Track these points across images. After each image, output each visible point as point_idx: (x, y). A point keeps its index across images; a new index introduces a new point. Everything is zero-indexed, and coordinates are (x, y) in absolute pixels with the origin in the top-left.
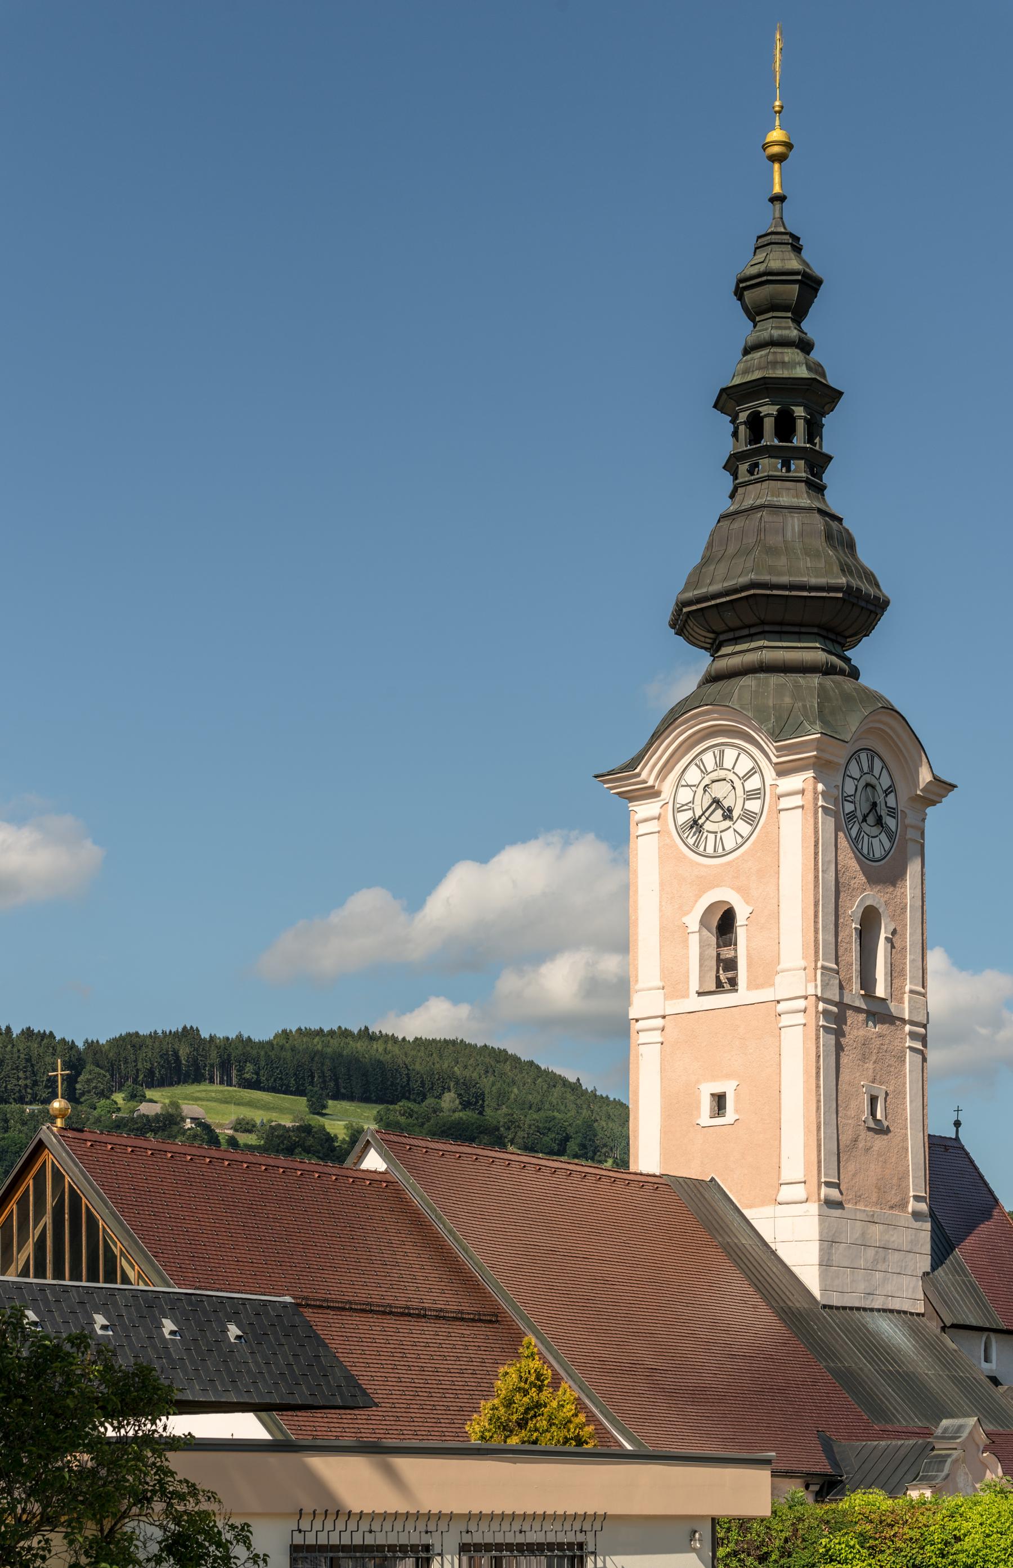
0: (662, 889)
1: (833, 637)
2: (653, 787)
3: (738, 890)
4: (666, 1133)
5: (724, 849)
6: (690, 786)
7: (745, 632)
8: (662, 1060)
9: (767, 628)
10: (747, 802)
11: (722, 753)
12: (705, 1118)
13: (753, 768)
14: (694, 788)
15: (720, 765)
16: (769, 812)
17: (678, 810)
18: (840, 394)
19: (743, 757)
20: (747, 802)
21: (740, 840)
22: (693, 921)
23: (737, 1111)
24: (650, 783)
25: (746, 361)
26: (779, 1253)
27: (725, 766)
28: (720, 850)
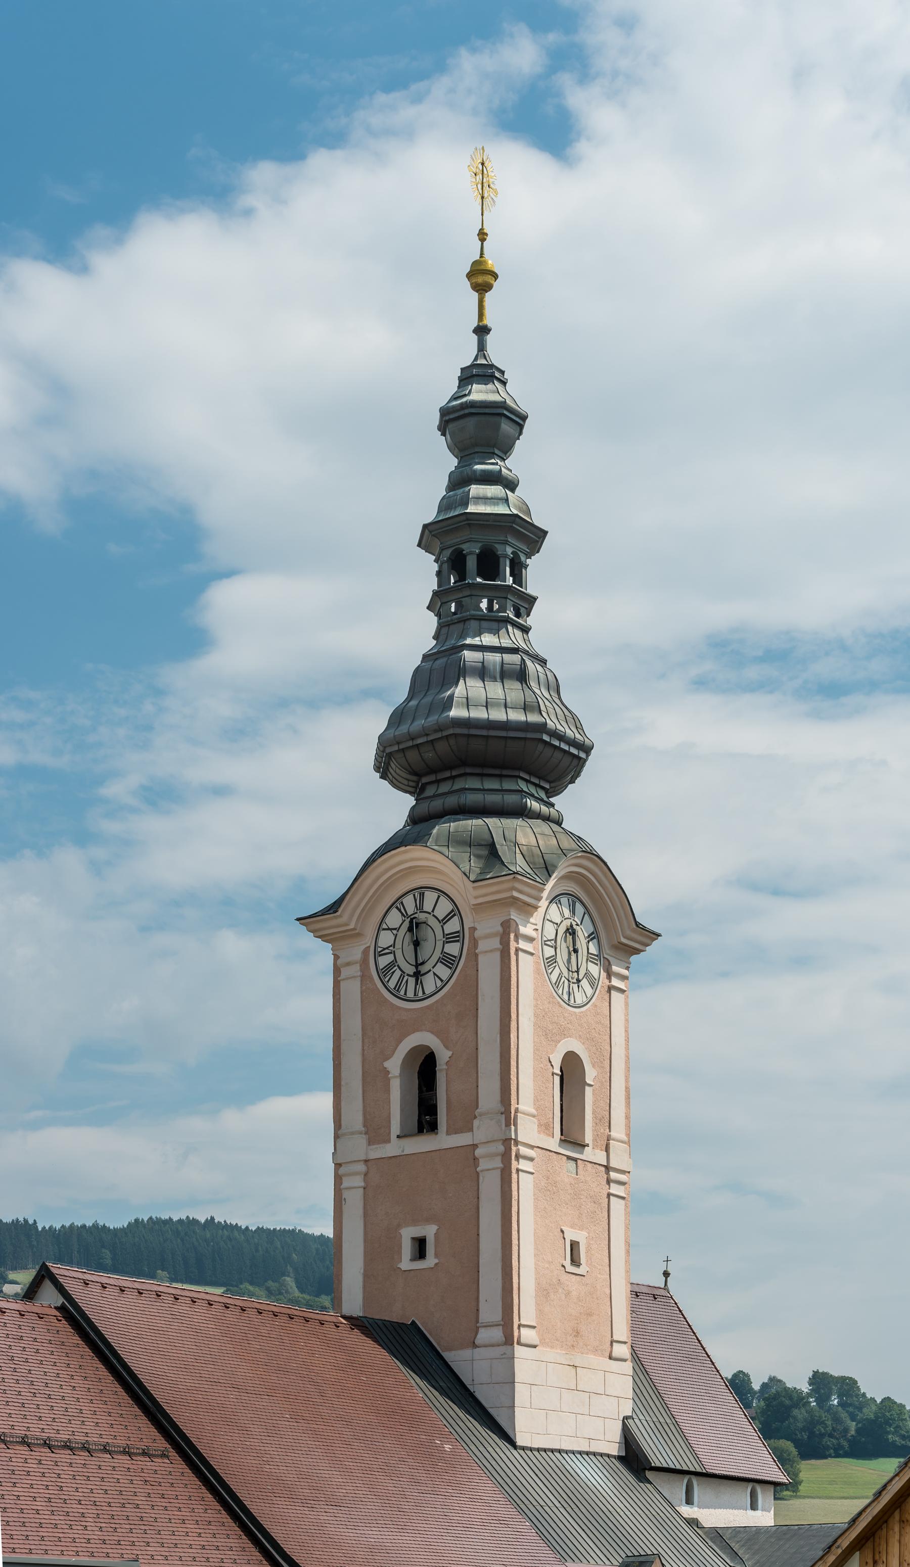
0: (364, 1034)
1: (537, 781)
2: (354, 929)
3: (437, 1034)
4: (368, 1276)
5: (424, 993)
6: (391, 929)
7: (447, 774)
9: (468, 770)
10: (446, 945)
11: (422, 895)
12: (406, 1263)
13: (452, 911)
14: (395, 932)
15: (420, 908)
16: (468, 954)
17: (379, 954)
18: (545, 533)
20: (446, 945)
21: (439, 984)
22: (394, 1065)
23: (436, 1256)
24: (352, 926)
25: (449, 497)
26: (477, 1395)
28: (420, 994)
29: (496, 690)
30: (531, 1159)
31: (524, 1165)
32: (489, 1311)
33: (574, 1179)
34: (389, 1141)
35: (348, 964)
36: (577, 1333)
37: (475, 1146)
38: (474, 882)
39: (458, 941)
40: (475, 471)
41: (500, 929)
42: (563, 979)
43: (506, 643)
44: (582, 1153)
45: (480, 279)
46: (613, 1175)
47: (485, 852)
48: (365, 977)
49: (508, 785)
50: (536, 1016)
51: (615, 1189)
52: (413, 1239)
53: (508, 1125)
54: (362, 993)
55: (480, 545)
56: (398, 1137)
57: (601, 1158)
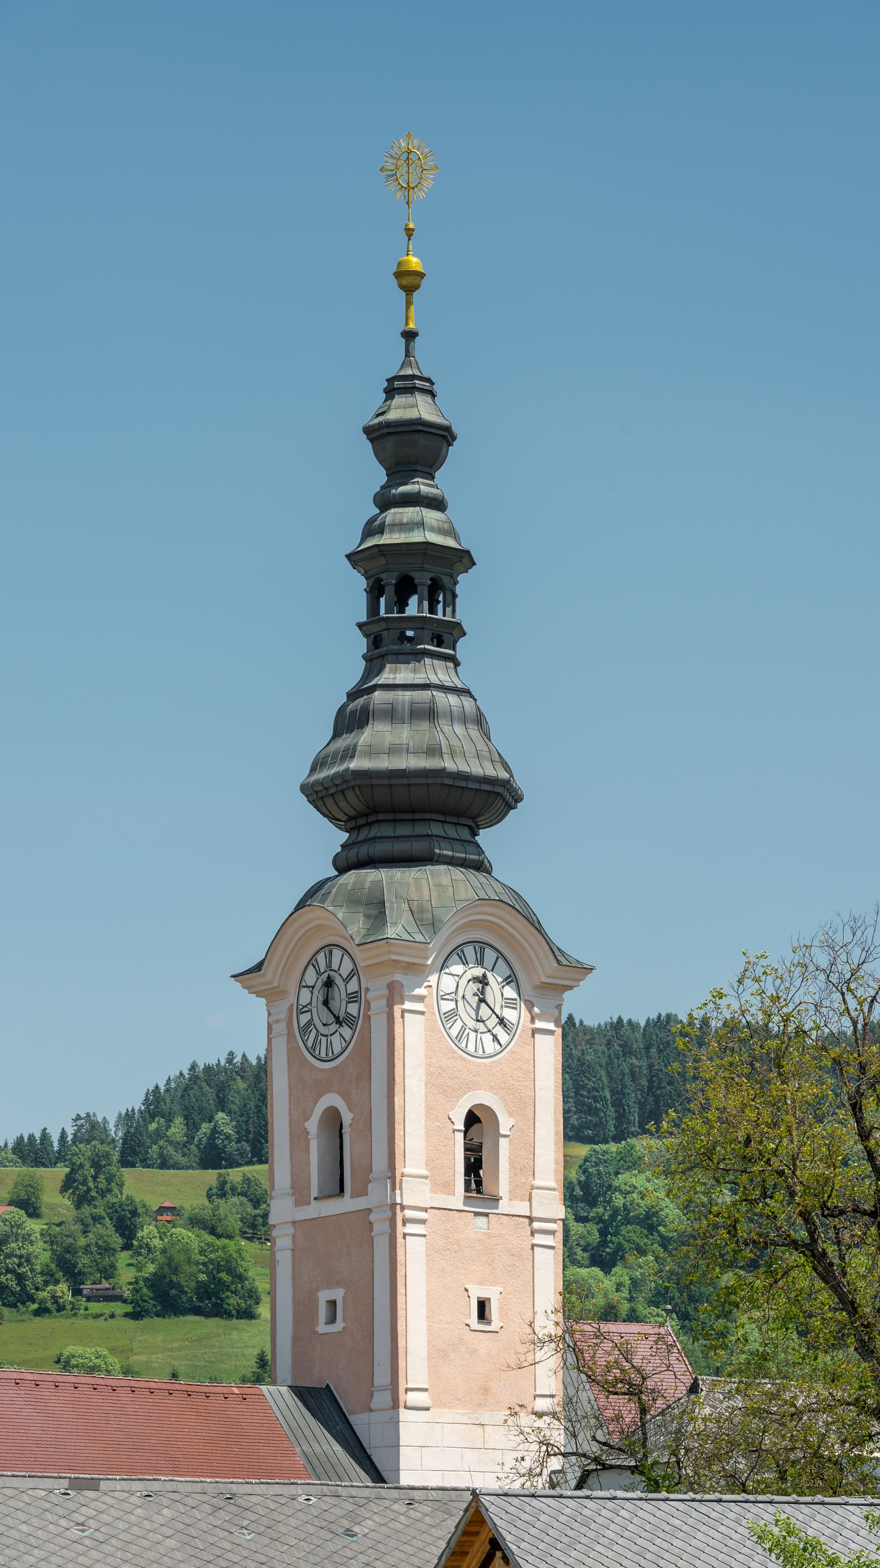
0: (290, 1094)
2: (278, 987)
4: (296, 1338)
8: (294, 1266)
11: (331, 953)
15: (329, 966)
16: (364, 1015)
19: (346, 958)
20: (349, 1005)
21: (344, 1044)
22: (312, 1125)
23: (344, 1320)
24: (275, 985)
26: (374, 1458)
27: (333, 968)
28: (330, 1054)
29: (404, 734)
30: (423, 1222)
31: (410, 1228)
32: (381, 1377)
33: (484, 1234)
34: (309, 1203)
35: (277, 1021)
36: (486, 1391)
37: (369, 1211)
38: (358, 945)
39: (356, 1001)
40: (394, 495)
41: (385, 992)
42: (467, 1031)
43: (419, 678)
44: (497, 1208)
45: (405, 281)
46: (536, 1225)
47: (374, 912)
48: (290, 1035)
49: (420, 829)
50: (428, 1074)
51: (539, 1239)
52: (328, 1302)
53: (393, 1189)
54: (288, 1051)
55: (397, 574)
56: (315, 1199)
57: (522, 1208)
